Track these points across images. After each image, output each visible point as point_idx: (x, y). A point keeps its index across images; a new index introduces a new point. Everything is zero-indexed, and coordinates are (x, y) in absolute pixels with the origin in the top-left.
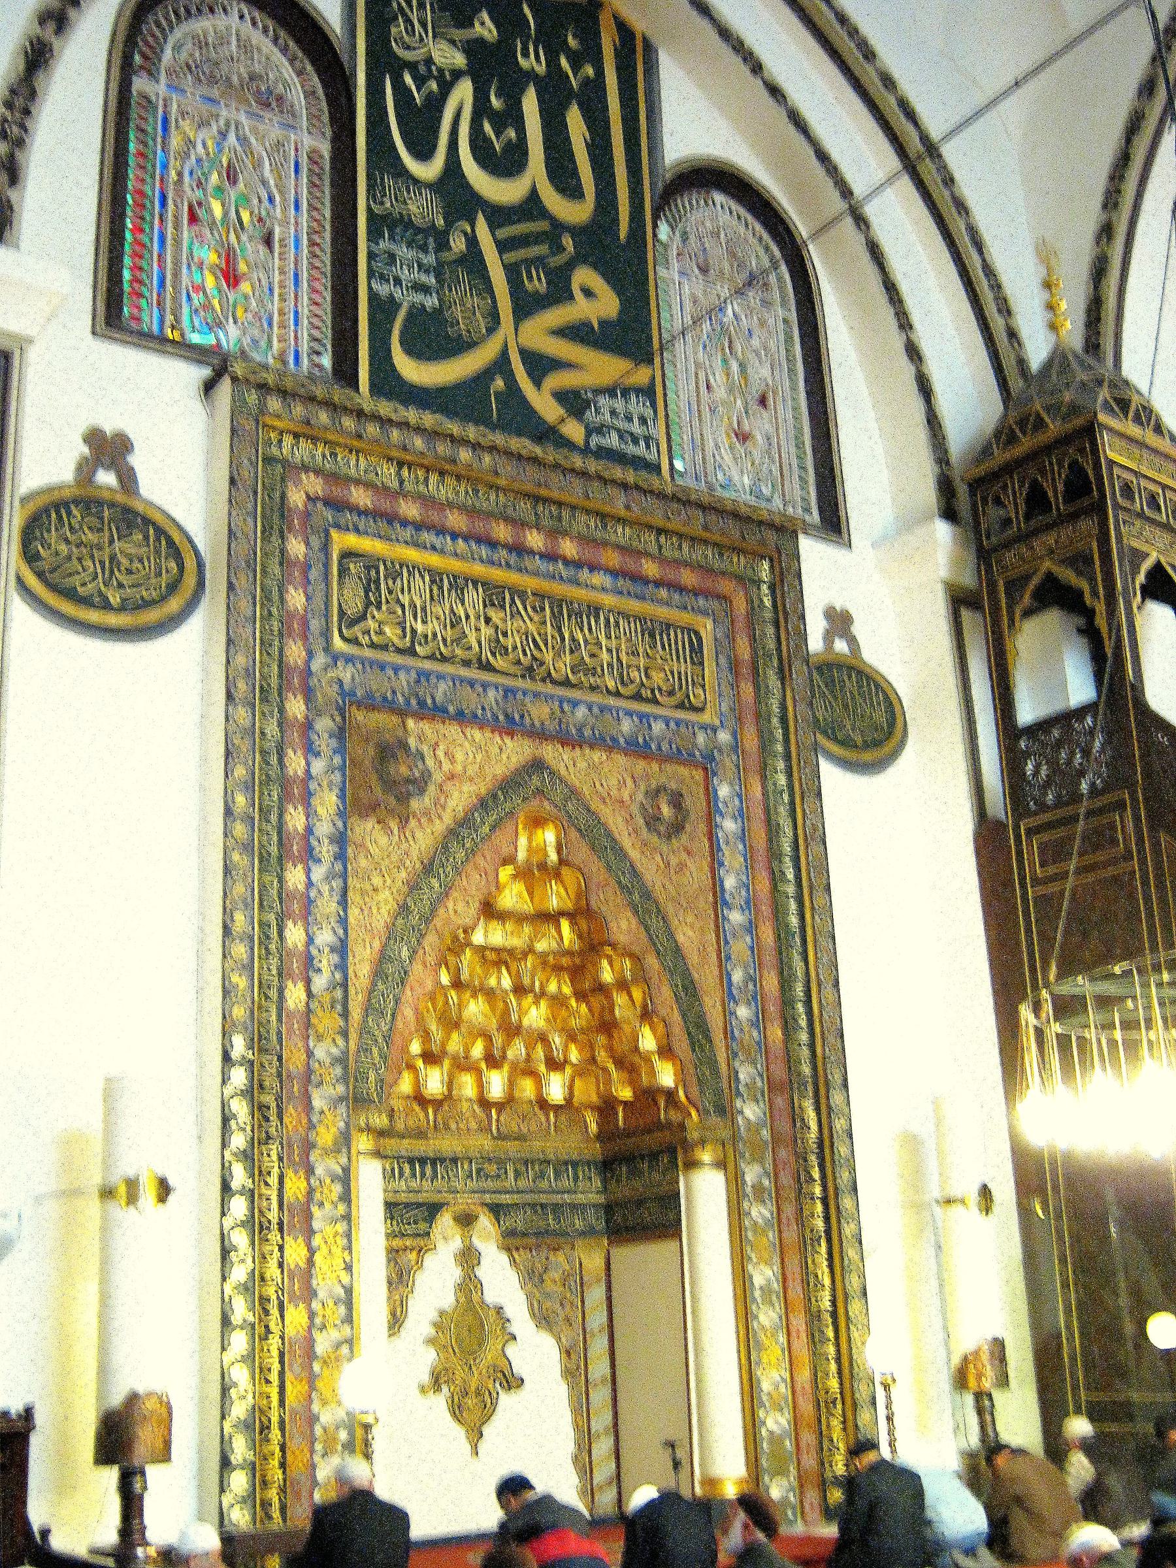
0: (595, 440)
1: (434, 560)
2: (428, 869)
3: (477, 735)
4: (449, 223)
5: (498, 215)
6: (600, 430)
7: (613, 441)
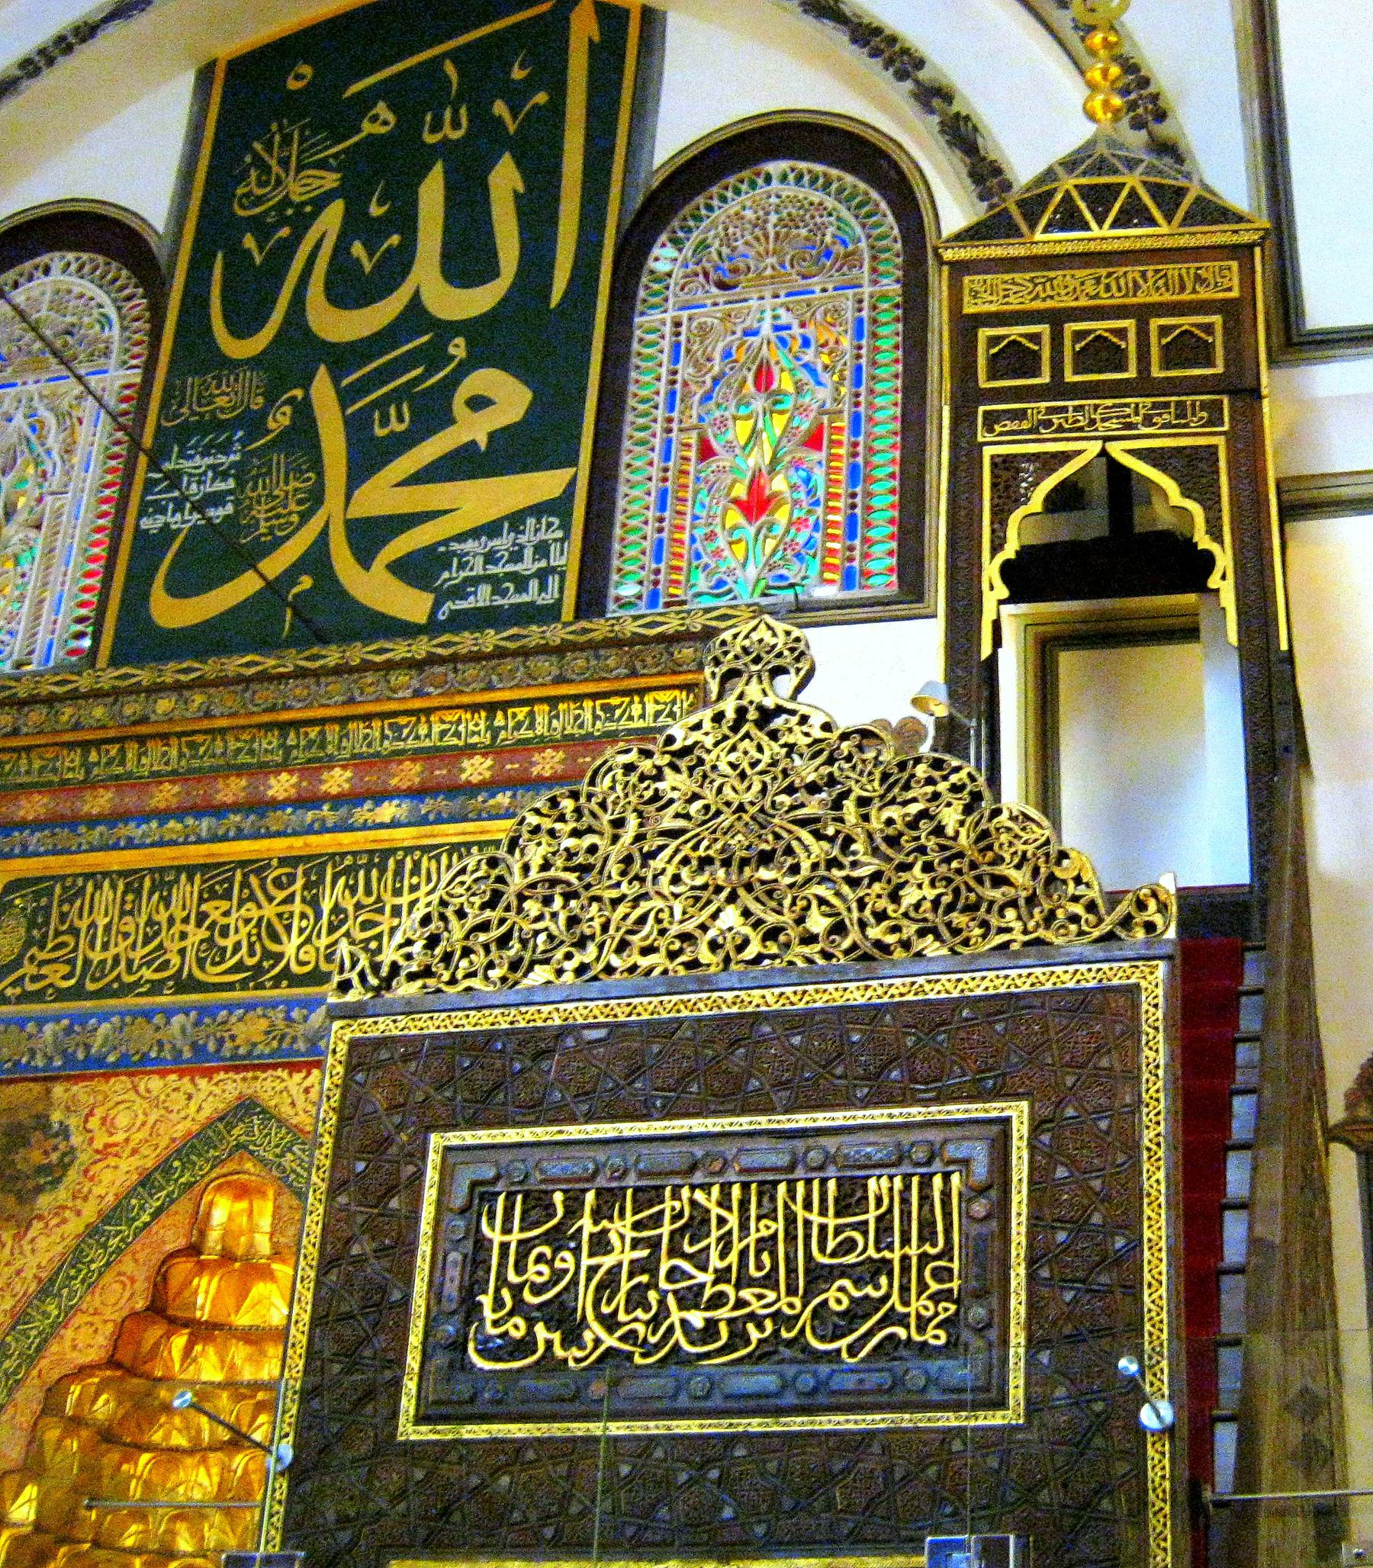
0: (449, 606)
1: (116, 860)
2: (46, 1289)
3: (155, 1083)
4: (271, 400)
5: (341, 357)
6: (459, 592)
7: (483, 597)
